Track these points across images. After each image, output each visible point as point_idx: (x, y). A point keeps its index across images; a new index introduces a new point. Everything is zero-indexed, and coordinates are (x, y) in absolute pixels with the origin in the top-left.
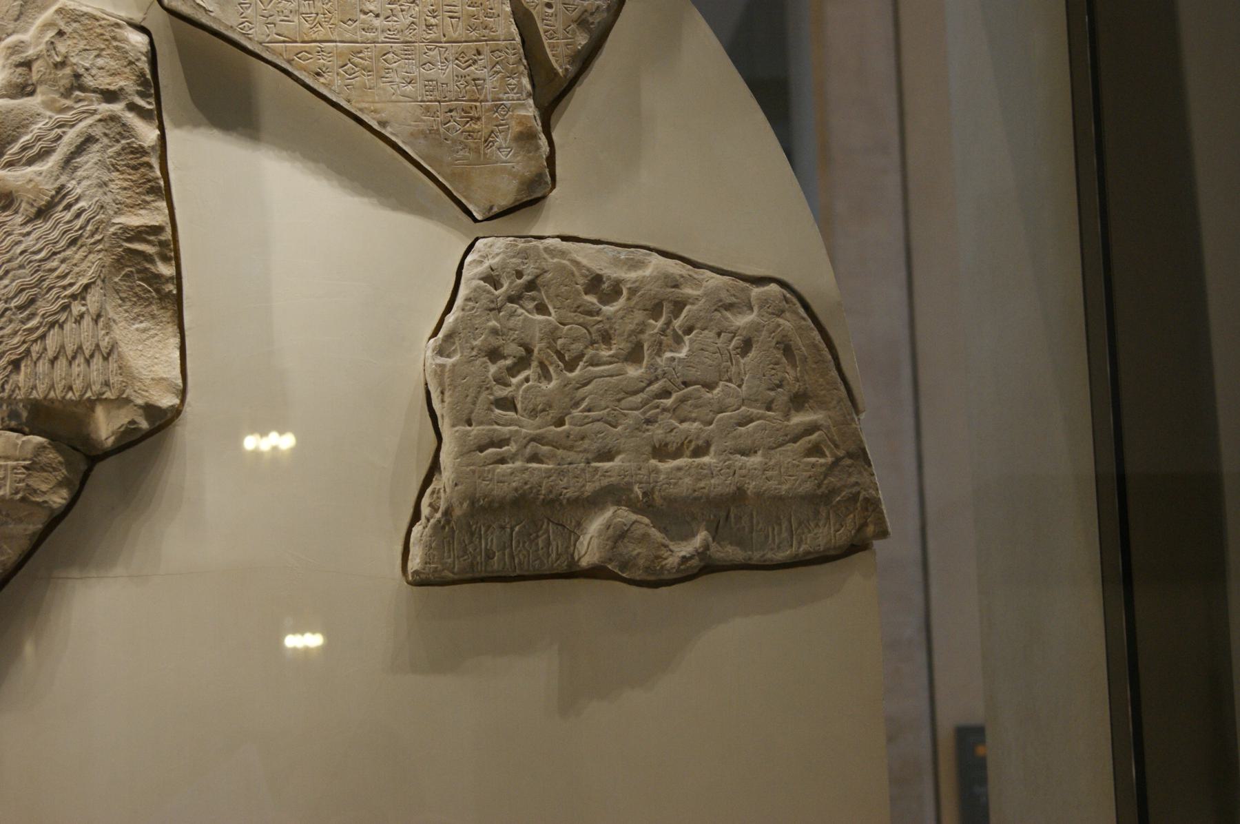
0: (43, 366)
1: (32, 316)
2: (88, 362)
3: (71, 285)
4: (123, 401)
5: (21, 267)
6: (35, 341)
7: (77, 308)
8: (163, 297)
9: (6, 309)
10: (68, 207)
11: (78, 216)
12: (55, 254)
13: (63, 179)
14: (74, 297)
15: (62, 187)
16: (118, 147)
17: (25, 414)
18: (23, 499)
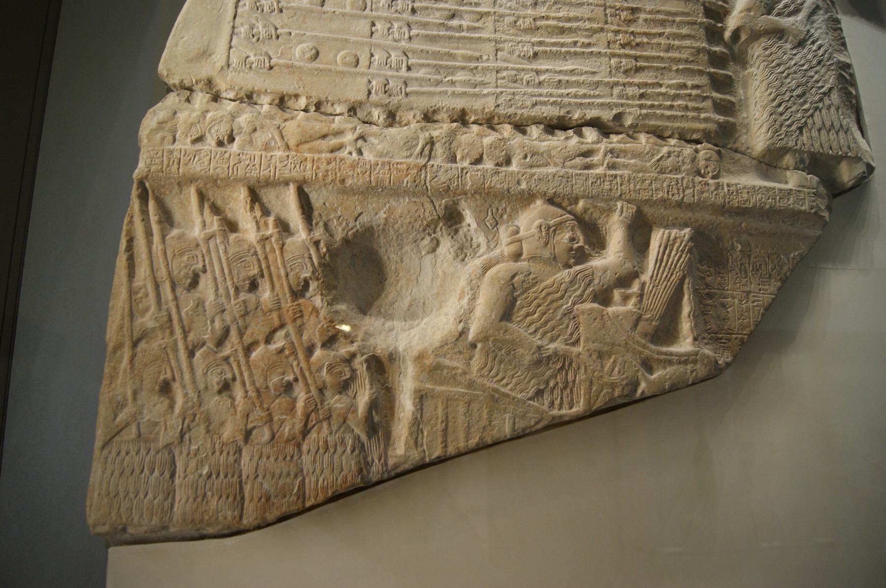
0: (814, 133)
1: (805, 102)
2: (837, 133)
3: (823, 87)
4: (858, 159)
5: (795, 73)
6: (808, 117)
7: (827, 101)
8: (852, 106)
9: (792, 96)
10: (813, 43)
11: (819, 48)
12: (811, 68)
13: (808, 27)
14: (824, 94)
15: (808, 31)
16: (826, 16)
17: (807, 161)
18: (816, 213)
